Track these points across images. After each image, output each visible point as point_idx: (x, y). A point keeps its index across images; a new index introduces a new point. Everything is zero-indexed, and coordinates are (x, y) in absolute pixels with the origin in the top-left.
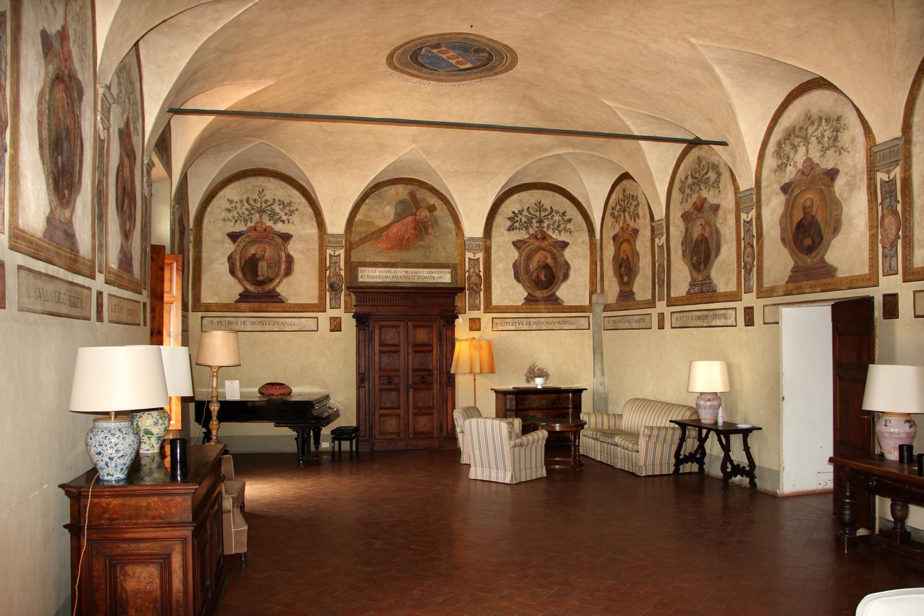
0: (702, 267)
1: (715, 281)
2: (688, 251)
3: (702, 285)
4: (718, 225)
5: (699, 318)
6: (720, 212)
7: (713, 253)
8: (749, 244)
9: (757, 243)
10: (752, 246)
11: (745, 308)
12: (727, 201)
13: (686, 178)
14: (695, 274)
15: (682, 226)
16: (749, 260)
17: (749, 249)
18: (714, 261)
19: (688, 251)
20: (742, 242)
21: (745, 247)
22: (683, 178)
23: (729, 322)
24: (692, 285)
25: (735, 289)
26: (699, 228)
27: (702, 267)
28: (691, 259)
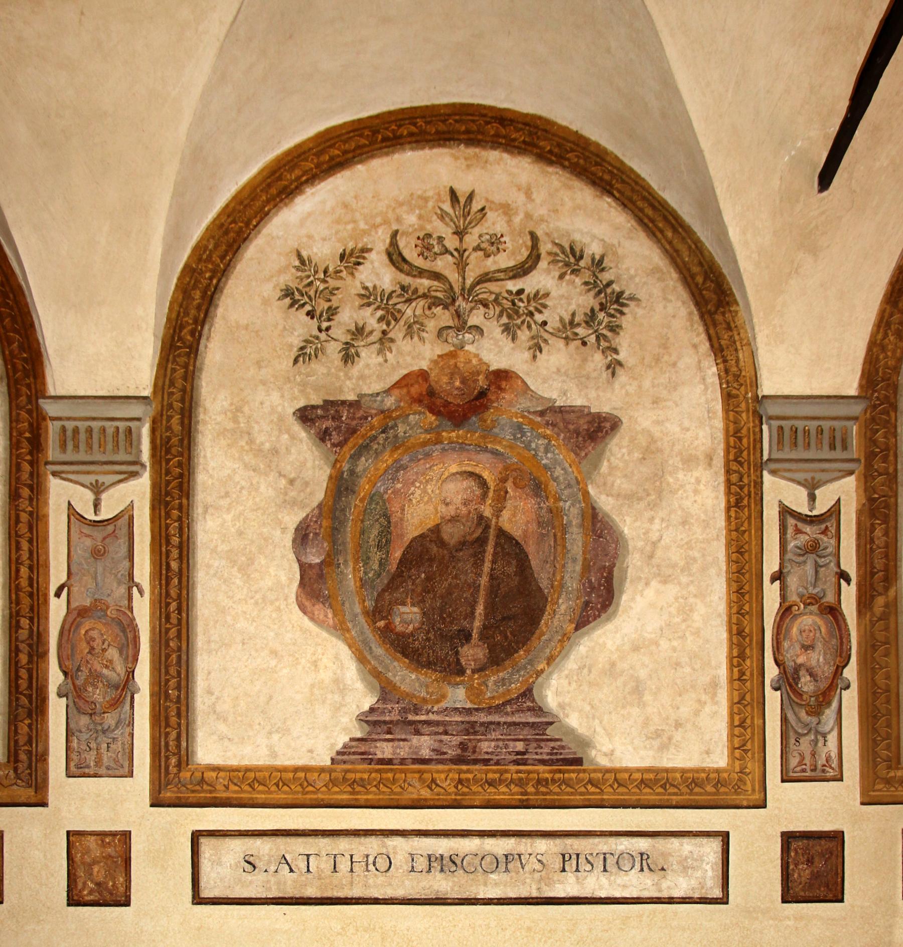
0: (472, 653)
1: (573, 721)
2: (350, 576)
3: (471, 728)
4: (605, 503)
5: (449, 864)
6: (618, 451)
7: (562, 608)
8: (812, 600)
9: (864, 603)
10: (833, 612)
11: (788, 838)
12: (670, 412)
13: (352, 258)
14: (407, 678)
15: (309, 464)
16: (817, 659)
17: (808, 621)
18: (565, 640)
19: (350, 576)
20: (771, 595)
21: (786, 611)
22: (324, 251)
23: (680, 886)
24: (374, 722)
25: (720, 759)
26: (458, 492)
27: (472, 653)
28: (378, 613)
